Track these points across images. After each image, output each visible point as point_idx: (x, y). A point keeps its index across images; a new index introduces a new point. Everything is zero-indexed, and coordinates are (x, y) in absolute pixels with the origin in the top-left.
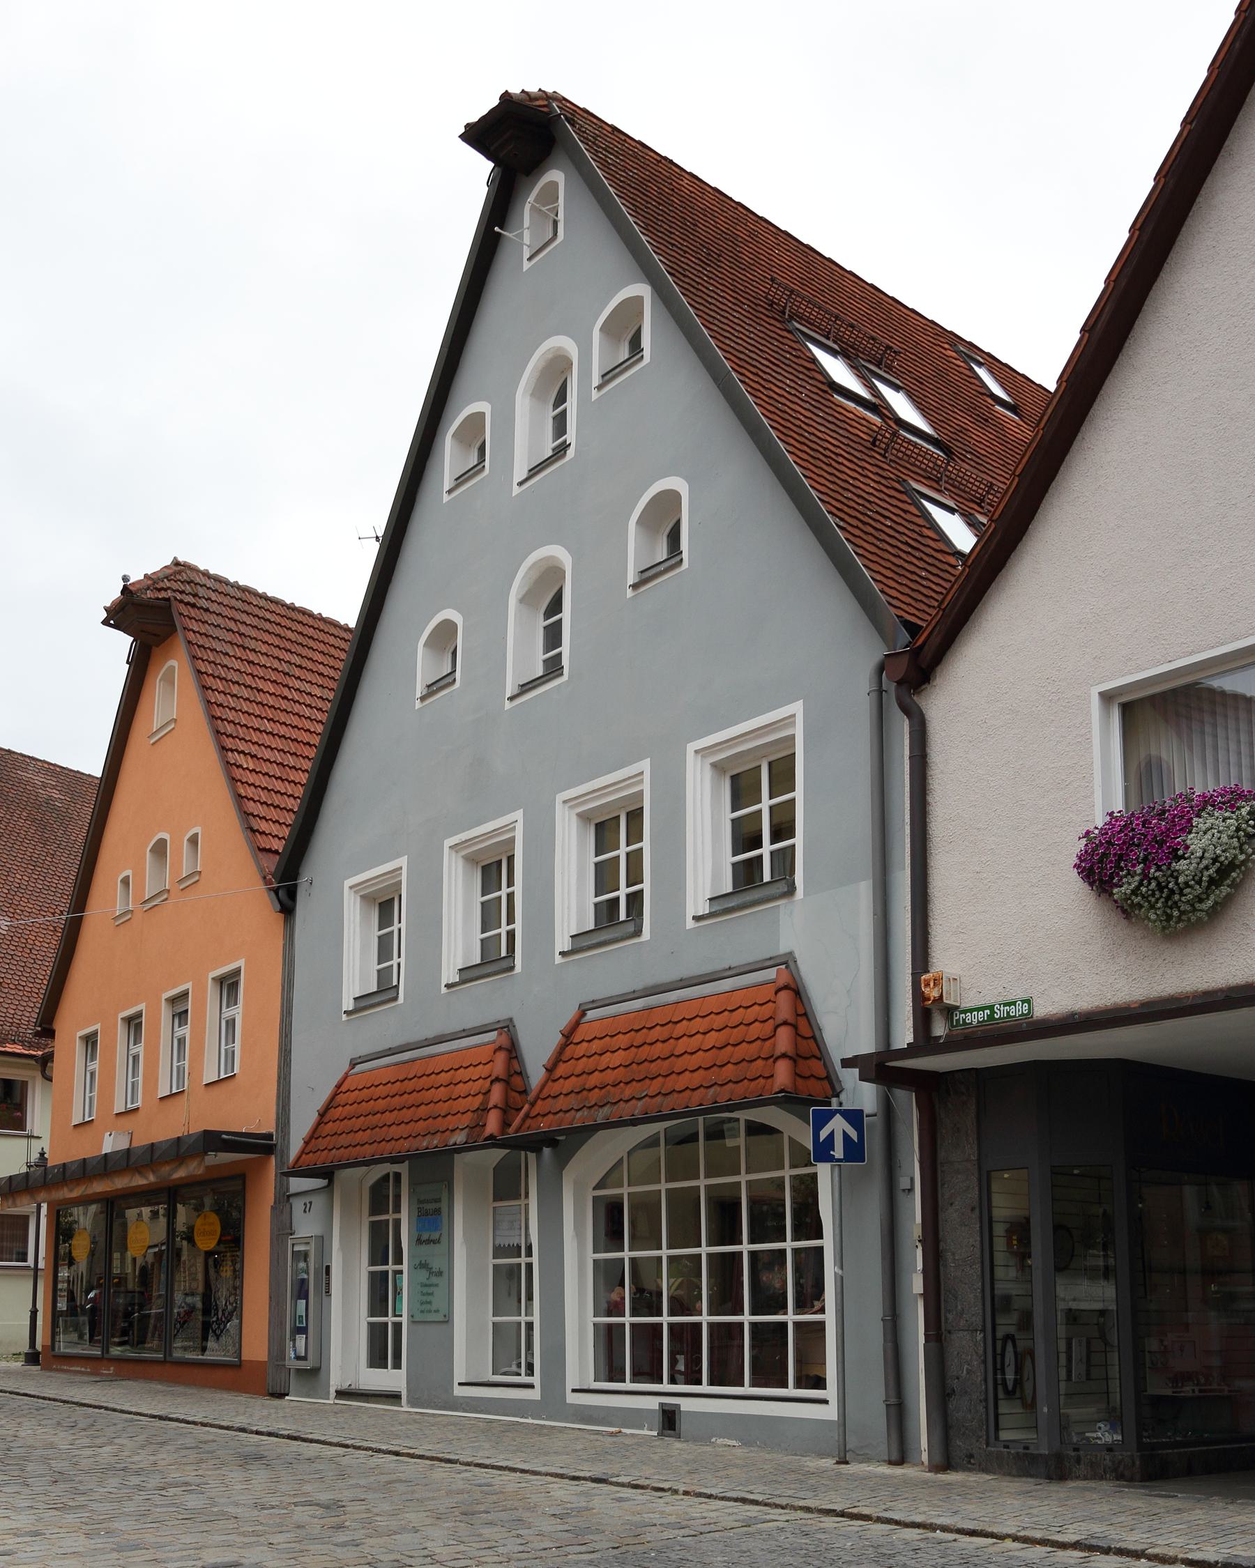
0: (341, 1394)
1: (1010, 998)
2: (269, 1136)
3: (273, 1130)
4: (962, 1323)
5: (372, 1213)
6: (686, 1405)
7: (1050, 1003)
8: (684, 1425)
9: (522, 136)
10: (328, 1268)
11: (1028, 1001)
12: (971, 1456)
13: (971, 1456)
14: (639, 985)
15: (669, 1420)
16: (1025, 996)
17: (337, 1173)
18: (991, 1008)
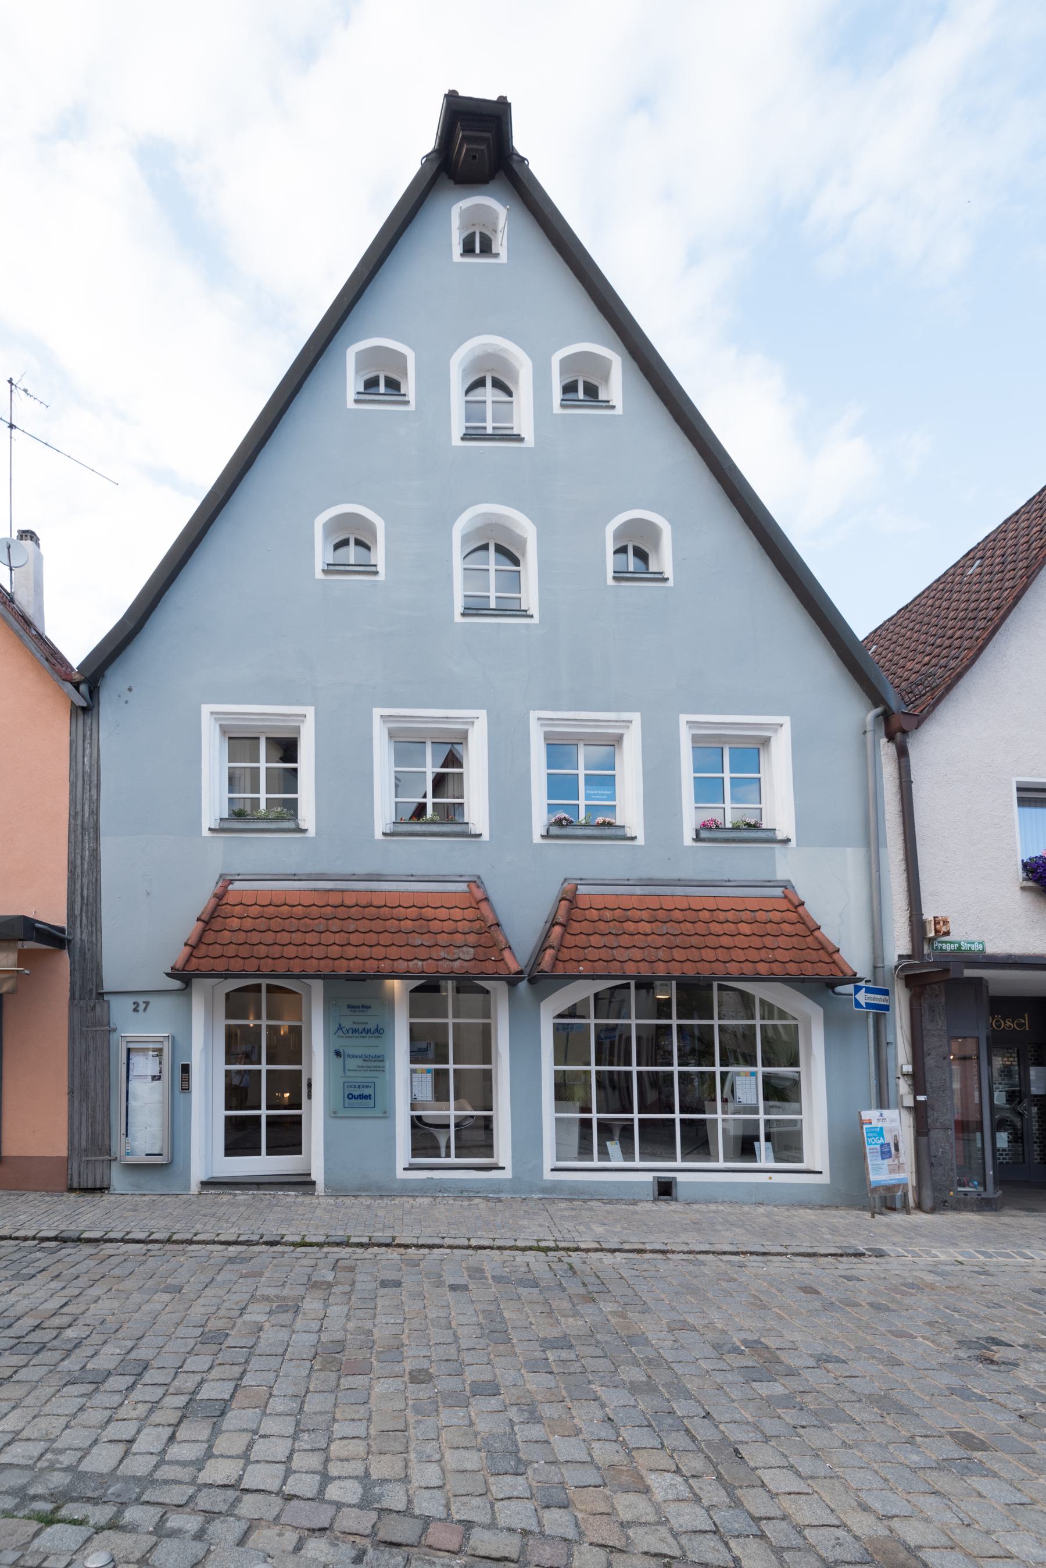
0: (205, 1184)
1: (970, 939)
2: (62, 930)
3: (65, 925)
4: (938, 1124)
5: (229, 1016)
6: (681, 1177)
7: (996, 947)
8: (680, 1192)
9: (475, 145)
10: (186, 1069)
11: (982, 943)
12: (946, 1202)
13: (946, 1202)
14: (634, 875)
15: (665, 1189)
16: (981, 940)
17: (194, 980)
18: (959, 943)
